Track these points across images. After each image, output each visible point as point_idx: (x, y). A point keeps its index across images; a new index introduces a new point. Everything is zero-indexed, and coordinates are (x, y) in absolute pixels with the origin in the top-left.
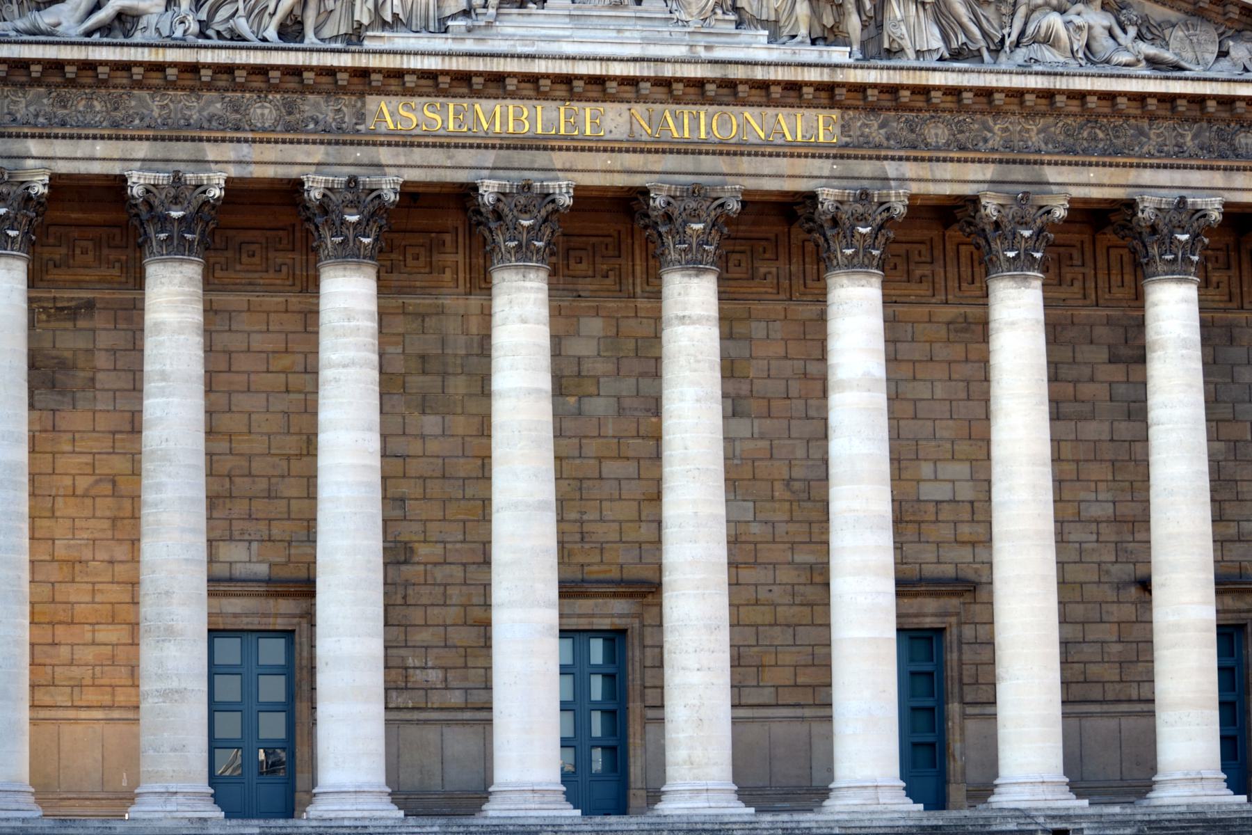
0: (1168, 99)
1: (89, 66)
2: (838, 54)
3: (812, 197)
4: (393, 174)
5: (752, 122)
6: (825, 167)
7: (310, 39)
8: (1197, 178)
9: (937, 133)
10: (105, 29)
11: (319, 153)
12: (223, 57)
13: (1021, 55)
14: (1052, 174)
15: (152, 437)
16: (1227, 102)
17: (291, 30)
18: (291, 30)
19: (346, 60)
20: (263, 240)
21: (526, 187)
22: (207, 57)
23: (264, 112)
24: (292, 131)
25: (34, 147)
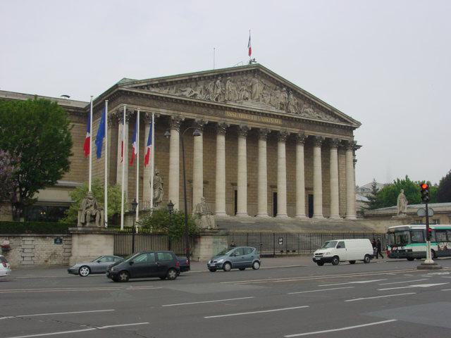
0: (320, 122)
1: (190, 102)
2: (284, 112)
3: (278, 132)
4: (229, 122)
5: (272, 120)
6: (280, 127)
7: (219, 101)
8: (322, 133)
9: (293, 124)
10: (192, 96)
11: (219, 119)
12: (209, 103)
13: (303, 115)
14: (306, 131)
15: (195, 158)
16: (326, 123)
17: (217, 99)
18: (217, 99)
19: (225, 105)
20: (210, 131)
21: (246, 126)
22: (207, 102)
23: (212, 112)
24: (216, 115)
25: (182, 113)
